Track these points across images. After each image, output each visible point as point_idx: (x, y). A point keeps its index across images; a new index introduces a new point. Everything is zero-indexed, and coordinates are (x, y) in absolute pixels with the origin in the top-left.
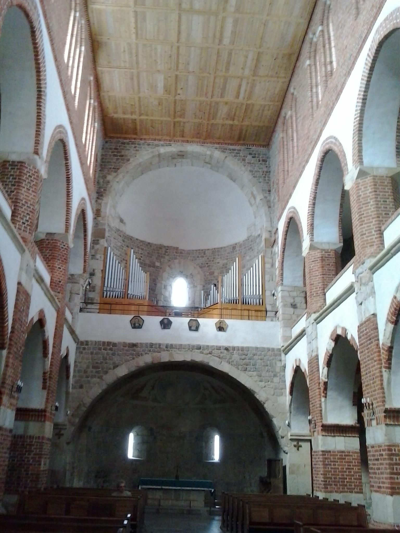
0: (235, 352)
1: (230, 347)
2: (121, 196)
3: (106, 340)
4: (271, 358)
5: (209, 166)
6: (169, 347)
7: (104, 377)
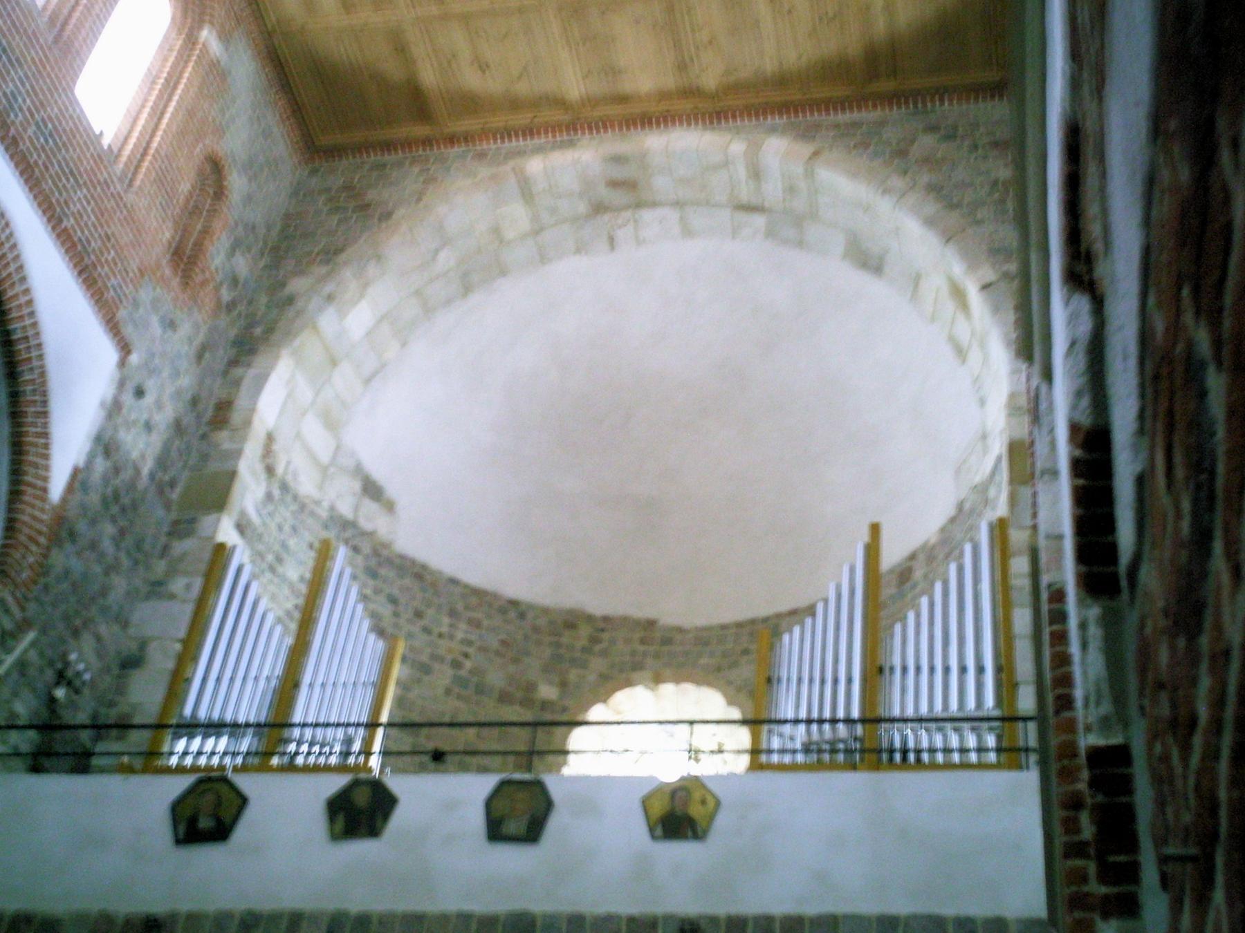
2: (368, 381)
5: (759, 221)
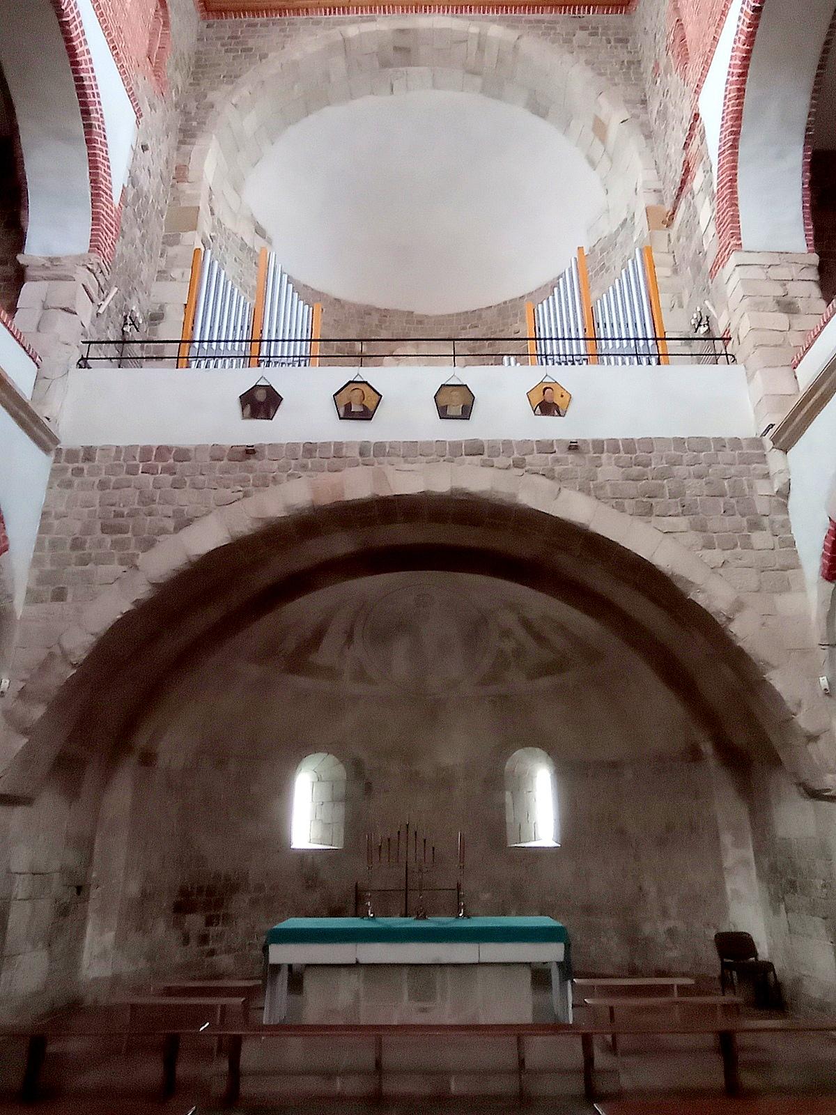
0: (604, 456)
1: (585, 441)
3: (155, 442)
4: (733, 470)
5: (478, 81)
6: (371, 453)
7: (142, 559)
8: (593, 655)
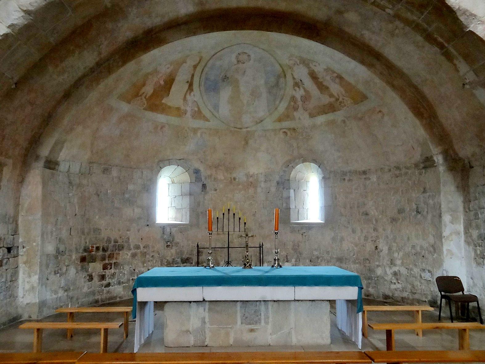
8: (360, 98)
